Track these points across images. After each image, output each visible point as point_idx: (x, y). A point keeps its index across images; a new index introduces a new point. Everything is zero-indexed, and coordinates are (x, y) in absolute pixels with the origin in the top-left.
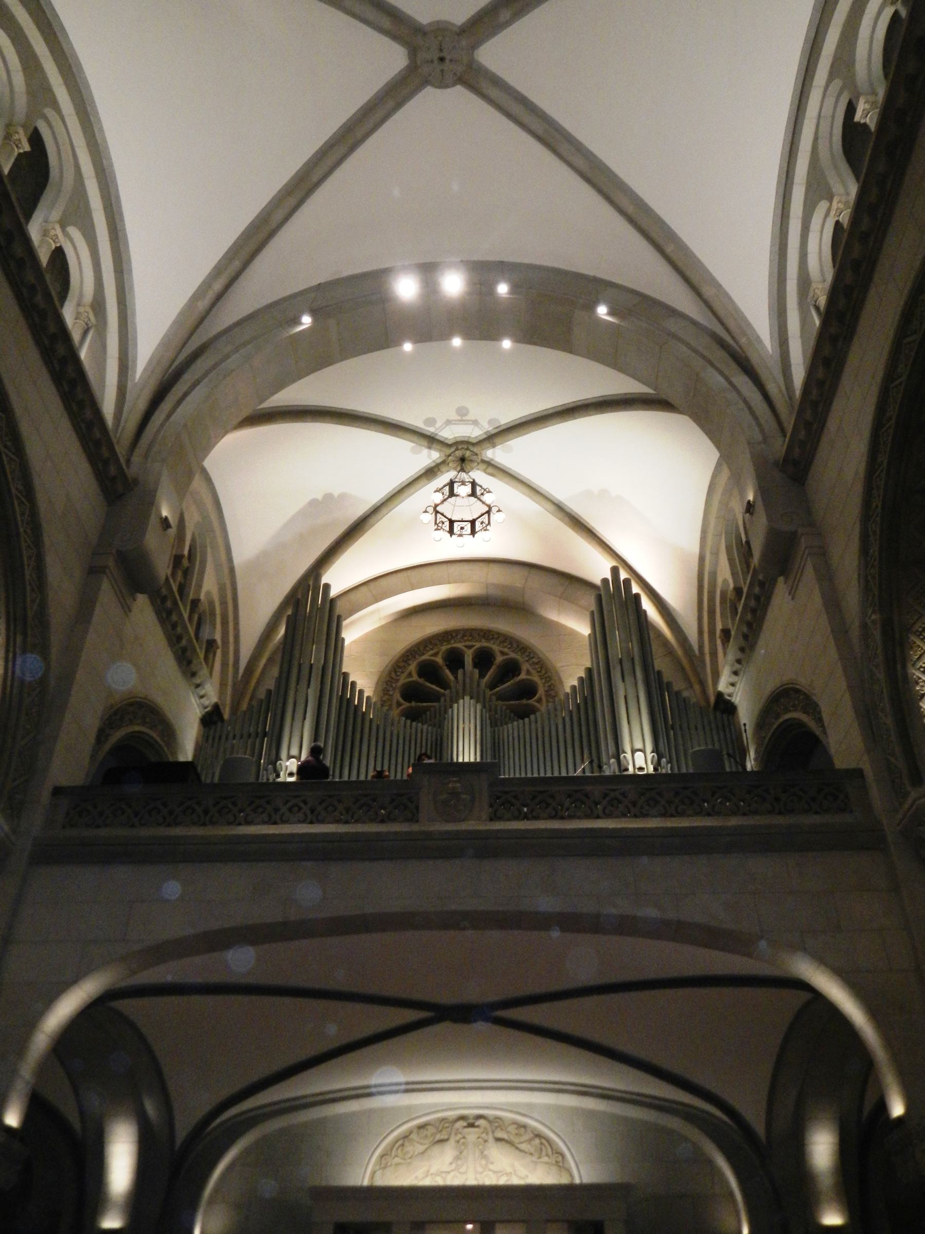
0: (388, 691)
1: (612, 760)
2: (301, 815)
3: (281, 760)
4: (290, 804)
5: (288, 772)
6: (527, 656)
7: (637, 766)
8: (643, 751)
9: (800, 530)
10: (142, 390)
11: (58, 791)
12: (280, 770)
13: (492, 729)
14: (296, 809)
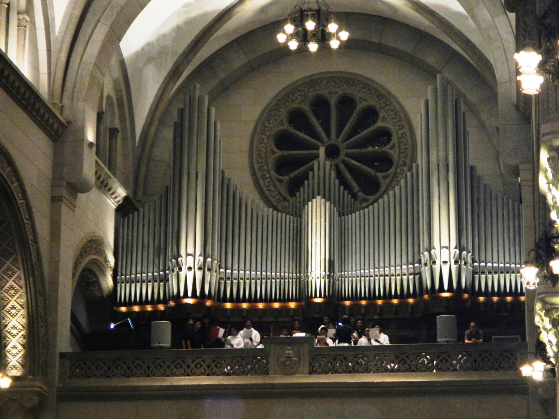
0: (264, 139)
1: (426, 253)
2: (202, 370)
3: (181, 256)
4: (195, 363)
5: (187, 267)
6: (384, 102)
7: (443, 260)
8: (448, 248)
9: (521, 167)
10: (62, 42)
11: (62, 355)
12: (181, 264)
13: (340, 218)
14: (199, 366)
